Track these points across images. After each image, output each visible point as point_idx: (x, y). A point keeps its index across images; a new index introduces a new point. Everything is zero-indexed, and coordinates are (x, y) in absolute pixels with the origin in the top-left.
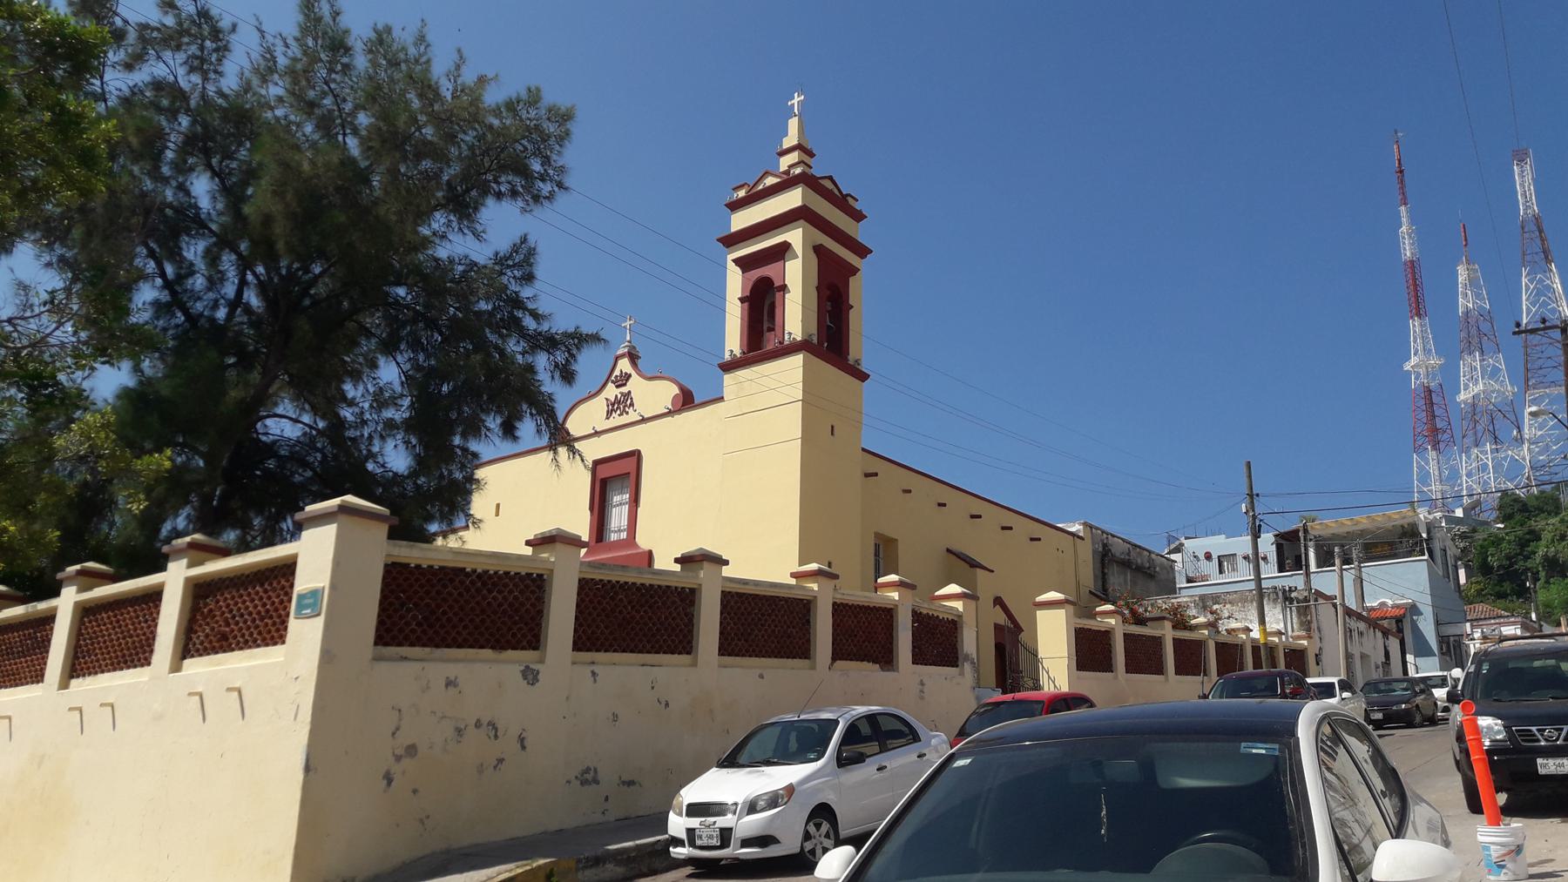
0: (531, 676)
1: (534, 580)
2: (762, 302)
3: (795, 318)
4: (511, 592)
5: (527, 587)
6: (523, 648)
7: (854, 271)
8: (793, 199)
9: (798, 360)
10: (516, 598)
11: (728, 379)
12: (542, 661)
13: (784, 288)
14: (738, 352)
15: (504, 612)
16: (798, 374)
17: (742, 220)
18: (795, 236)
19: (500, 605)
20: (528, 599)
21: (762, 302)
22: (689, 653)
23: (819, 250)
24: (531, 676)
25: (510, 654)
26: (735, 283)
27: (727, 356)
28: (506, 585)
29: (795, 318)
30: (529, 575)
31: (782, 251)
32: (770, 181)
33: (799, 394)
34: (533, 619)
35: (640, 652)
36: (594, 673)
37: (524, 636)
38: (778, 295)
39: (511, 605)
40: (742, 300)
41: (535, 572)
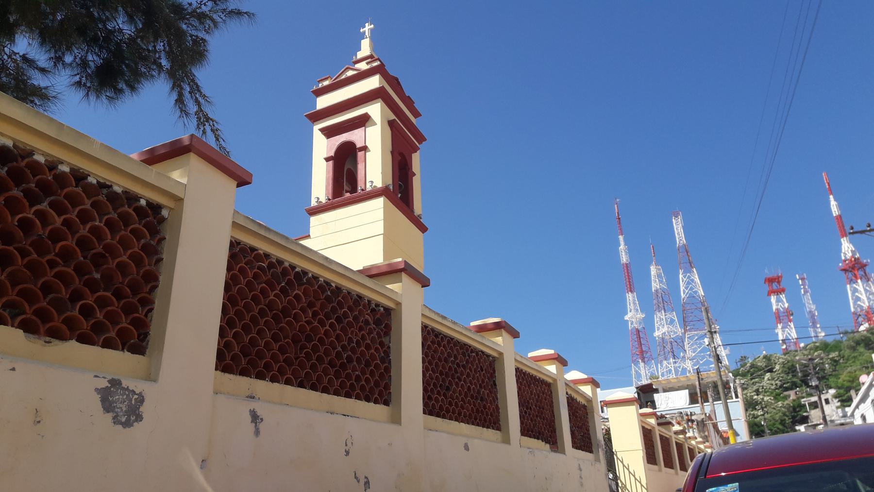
0: (122, 407)
1: (139, 210)
2: (345, 161)
3: (374, 170)
4: (84, 217)
5: (125, 219)
6: (107, 344)
7: (415, 149)
8: (374, 82)
9: (380, 202)
10: (95, 231)
11: (314, 220)
12: (151, 376)
13: (365, 149)
14: (323, 200)
15: (66, 255)
16: (380, 214)
17: (324, 102)
18: (375, 110)
19: (56, 236)
20: (124, 243)
21: (345, 161)
22: (386, 403)
23: (391, 124)
24: (122, 407)
25: (73, 347)
26: (322, 148)
27: (314, 203)
28: (74, 200)
29: (374, 170)
30: (131, 198)
31: (363, 121)
32: (350, 73)
33: (380, 228)
34: (135, 288)
35: (325, 390)
36: (255, 417)
37: (112, 317)
38: (360, 154)
39: (82, 243)
40: (327, 159)
41: (147, 195)
